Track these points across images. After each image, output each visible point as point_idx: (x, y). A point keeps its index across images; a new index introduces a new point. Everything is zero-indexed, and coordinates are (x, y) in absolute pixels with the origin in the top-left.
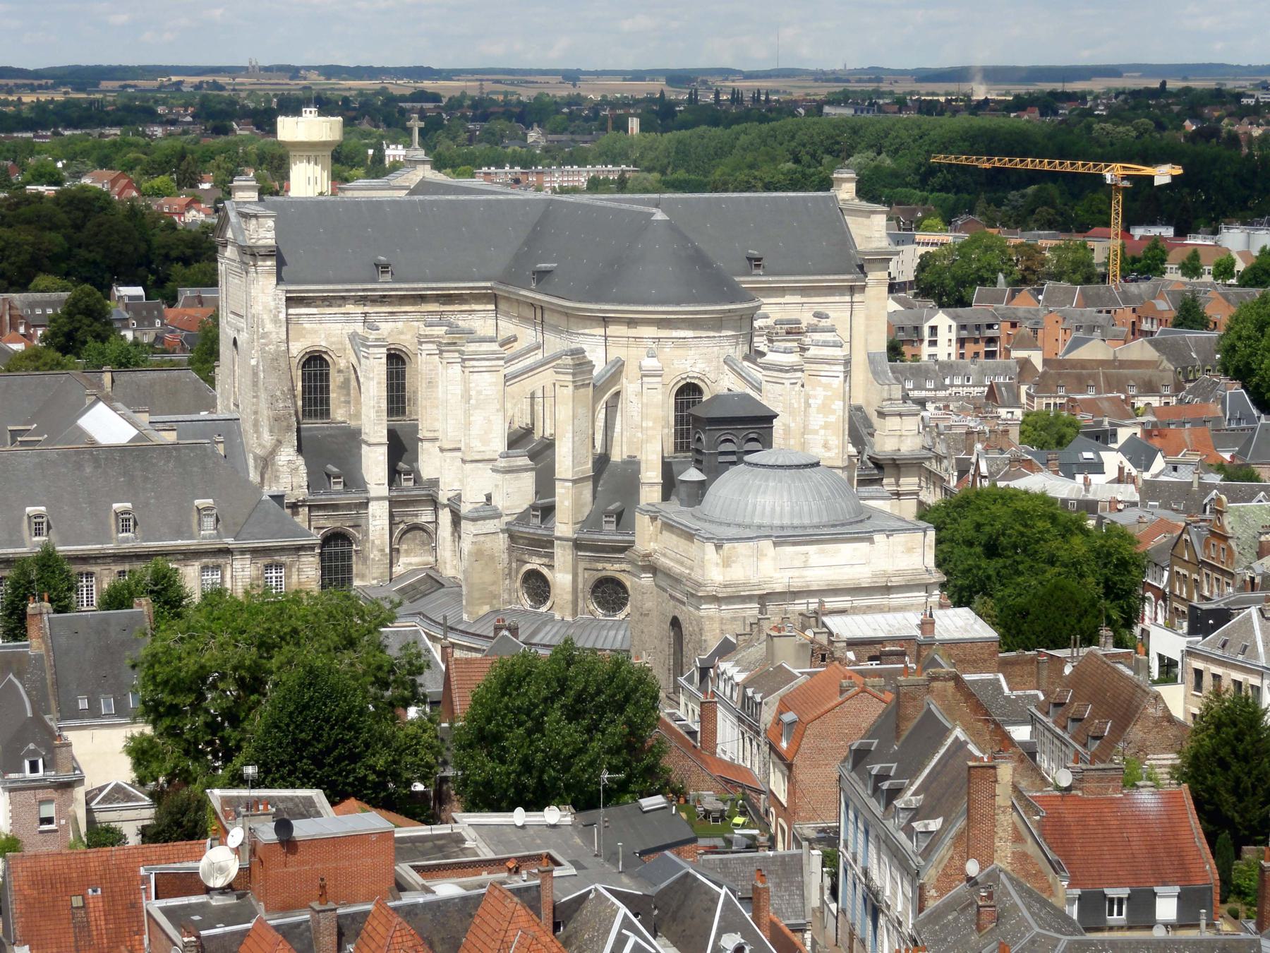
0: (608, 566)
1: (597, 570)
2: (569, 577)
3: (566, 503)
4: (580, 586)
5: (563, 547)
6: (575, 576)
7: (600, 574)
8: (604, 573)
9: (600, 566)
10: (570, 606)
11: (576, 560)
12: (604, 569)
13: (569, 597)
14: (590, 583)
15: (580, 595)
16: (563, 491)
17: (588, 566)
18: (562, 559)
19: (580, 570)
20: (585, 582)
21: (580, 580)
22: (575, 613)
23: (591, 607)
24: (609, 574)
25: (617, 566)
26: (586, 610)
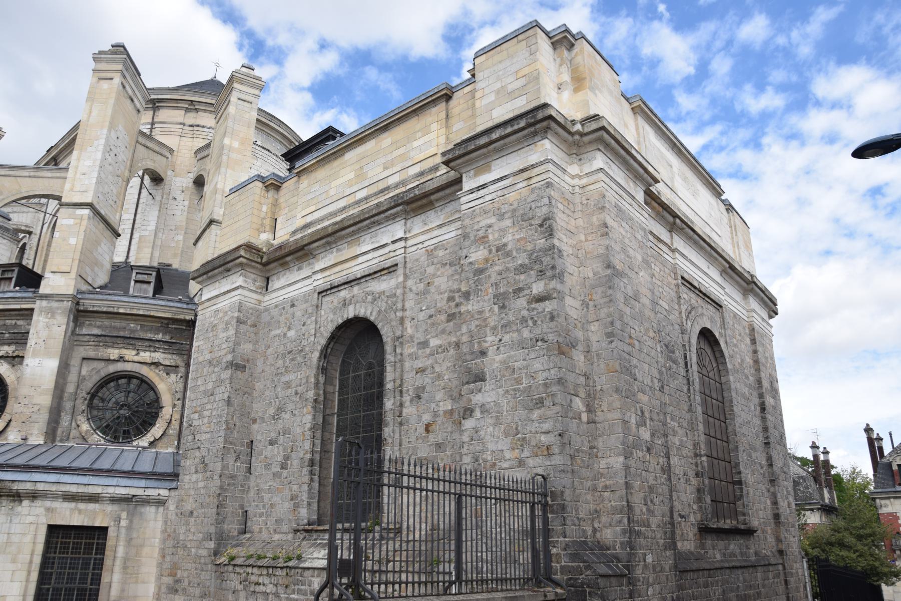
0: (130, 354)
1: (108, 360)
2: (52, 365)
3: (73, 241)
4: (70, 388)
5: (51, 313)
6: (64, 368)
7: (112, 368)
8: (120, 366)
9: (114, 353)
10: (44, 417)
11: (73, 339)
12: (121, 359)
13: (46, 400)
14: (89, 385)
15: (68, 405)
16: (71, 222)
17: (92, 354)
18: (44, 334)
19: (75, 361)
20: (81, 380)
21: (72, 377)
22: (51, 434)
23: (85, 427)
24: (128, 367)
25: (145, 356)
26: (74, 433)
